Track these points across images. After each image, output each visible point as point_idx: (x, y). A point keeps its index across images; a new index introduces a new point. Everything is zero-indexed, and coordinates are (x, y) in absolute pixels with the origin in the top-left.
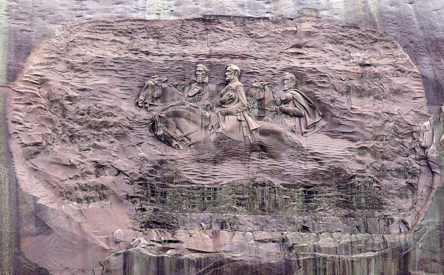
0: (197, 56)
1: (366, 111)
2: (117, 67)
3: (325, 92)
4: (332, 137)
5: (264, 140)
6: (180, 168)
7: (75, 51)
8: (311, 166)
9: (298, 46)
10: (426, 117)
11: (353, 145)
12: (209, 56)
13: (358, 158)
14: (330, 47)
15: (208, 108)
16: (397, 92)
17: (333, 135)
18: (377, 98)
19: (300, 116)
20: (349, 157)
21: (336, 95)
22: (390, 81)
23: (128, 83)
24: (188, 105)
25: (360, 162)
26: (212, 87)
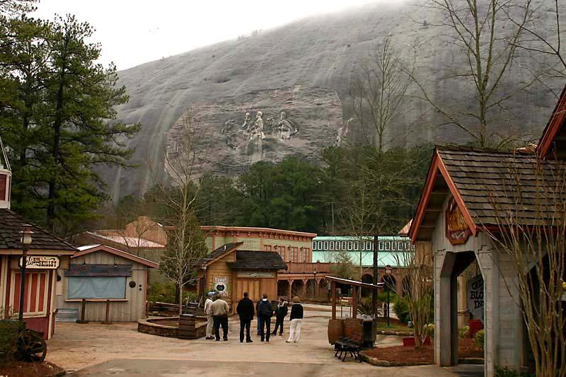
0: (247, 109)
1: (316, 126)
2: (214, 118)
3: (298, 119)
4: (302, 139)
5: (267, 143)
6: (235, 158)
7: (199, 113)
8: (289, 153)
9: (289, 100)
10: (341, 126)
11: (309, 142)
12: (251, 109)
13: (310, 147)
14: (305, 98)
15: (248, 131)
16: (330, 116)
17: (302, 138)
18: (322, 119)
19: (287, 131)
20: (306, 148)
21: (302, 119)
22: (328, 111)
23: (218, 124)
24: (240, 130)
25: (310, 149)
26: (251, 122)
